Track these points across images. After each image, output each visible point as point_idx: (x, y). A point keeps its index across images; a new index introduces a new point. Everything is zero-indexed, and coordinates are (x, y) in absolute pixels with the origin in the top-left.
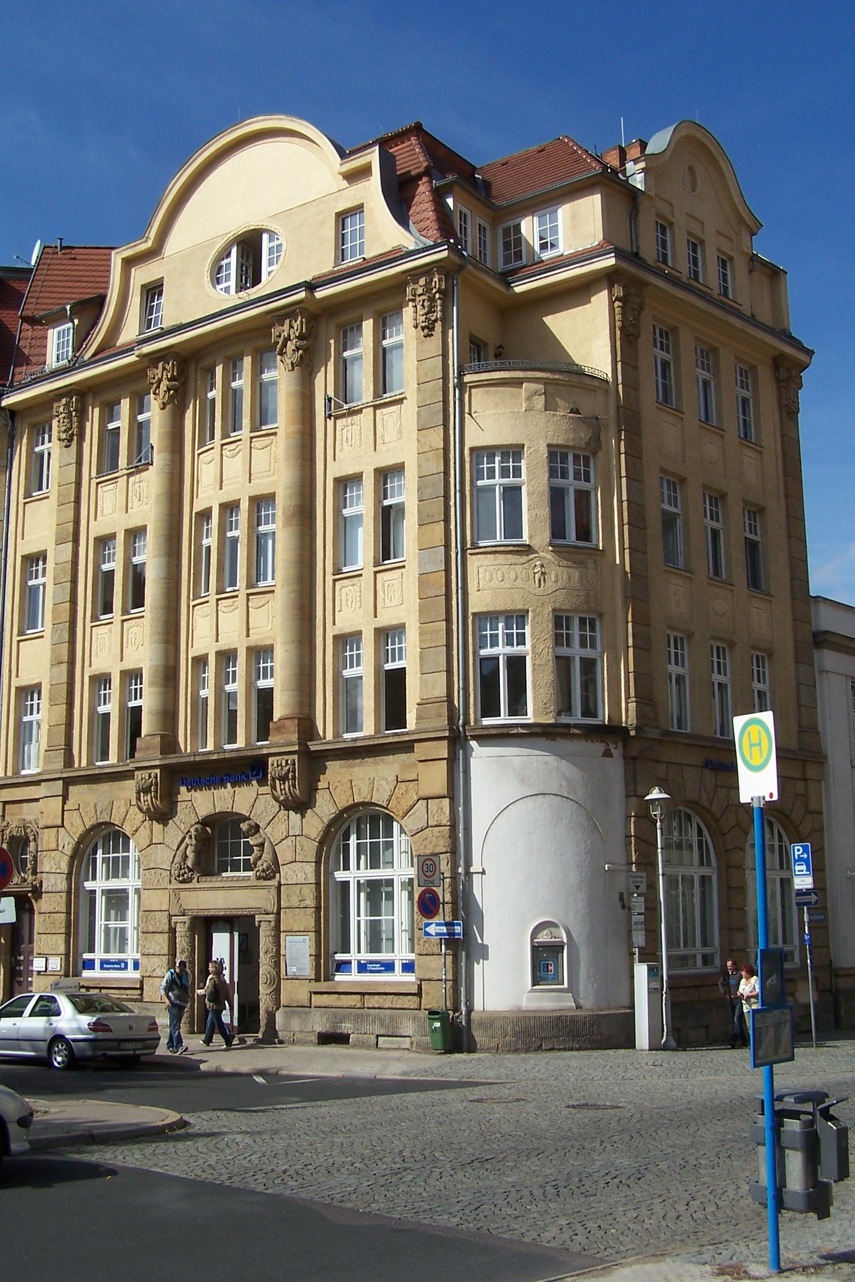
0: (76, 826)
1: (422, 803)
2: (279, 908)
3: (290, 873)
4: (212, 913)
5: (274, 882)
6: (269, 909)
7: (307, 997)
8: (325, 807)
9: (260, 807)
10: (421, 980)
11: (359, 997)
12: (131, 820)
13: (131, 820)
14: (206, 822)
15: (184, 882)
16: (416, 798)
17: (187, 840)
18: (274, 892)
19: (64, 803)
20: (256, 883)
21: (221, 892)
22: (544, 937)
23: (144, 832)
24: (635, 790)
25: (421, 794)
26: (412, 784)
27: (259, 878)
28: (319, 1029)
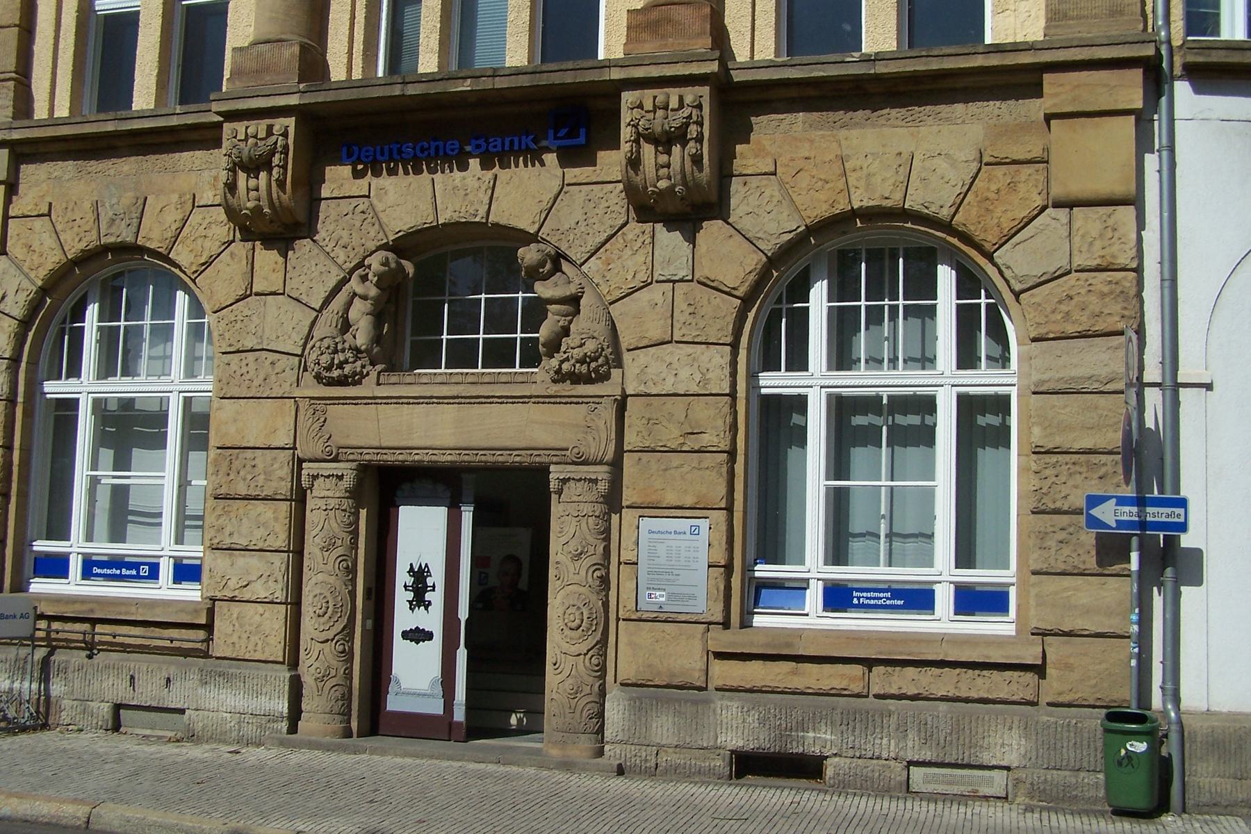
1: (1062, 214)
2: (620, 451)
5: (609, 388)
6: (592, 450)
11: (858, 670)
14: (402, 246)
17: (354, 284)
18: (608, 413)
20: (554, 389)
21: (450, 411)
25: (1057, 191)
27: (560, 377)
28: (734, 740)
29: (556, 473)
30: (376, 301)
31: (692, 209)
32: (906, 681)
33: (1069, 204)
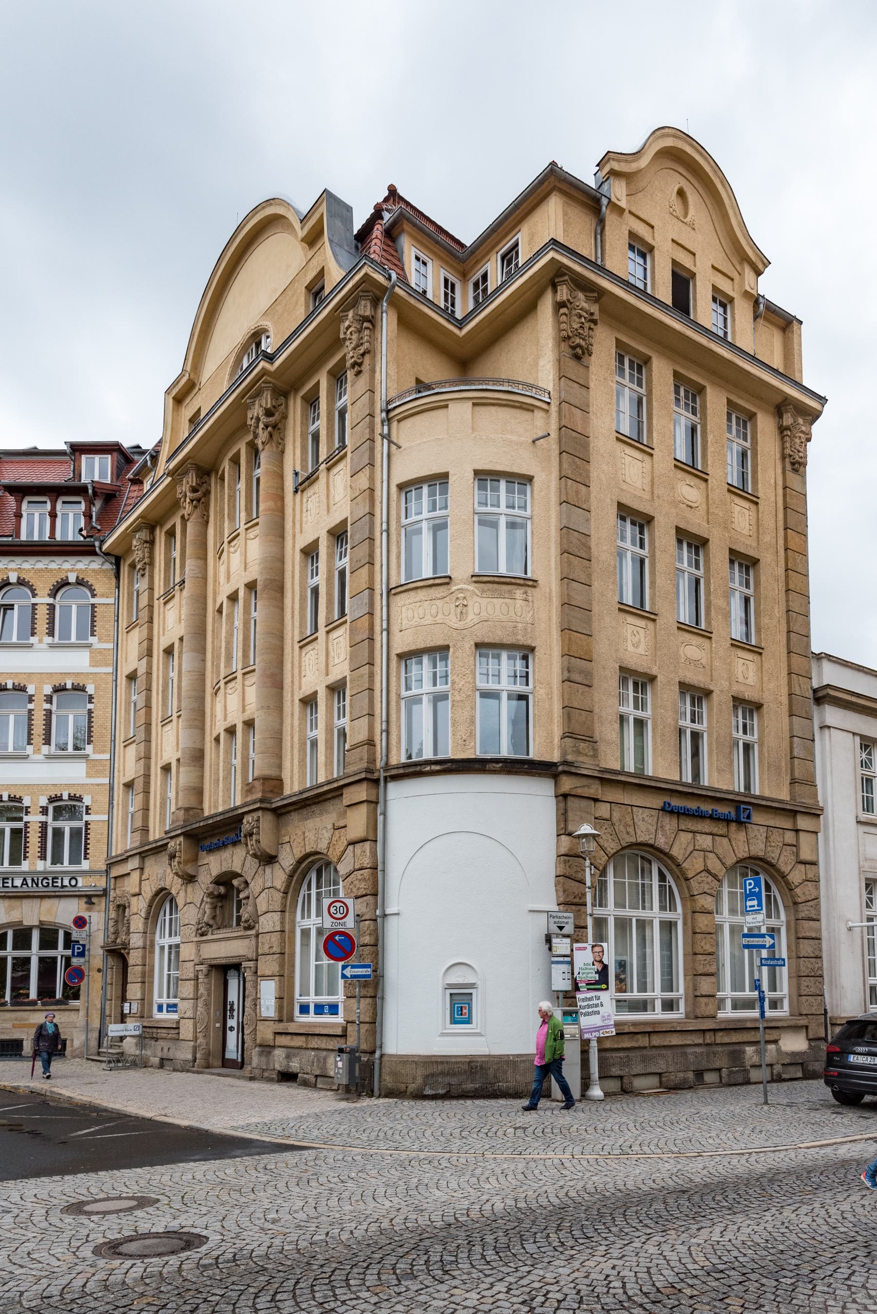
0: (148, 890)
1: (351, 847)
3: (265, 922)
4: (224, 961)
5: (253, 932)
6: (250, 956)
7: (272, 1037)
8: (287, 860)
9: (247, 864)
10: (348, 1022)
11: (303, 1038)
12: (175, 885)
13: (175, 885)
15: (202, 935)
16: (346, 843)
17: (205, 899)
18: (254, 941)
19: (142, 874)
22: (456, 978)
23: (182, 894)
24: (566, 828)
25: (349, 838)
26: (343, 830)
28: (278, 1067)
29: (244, 964)
30: (212, 903)
31: (268, 859)
32: (315, 1043)
33: (353, 843)
